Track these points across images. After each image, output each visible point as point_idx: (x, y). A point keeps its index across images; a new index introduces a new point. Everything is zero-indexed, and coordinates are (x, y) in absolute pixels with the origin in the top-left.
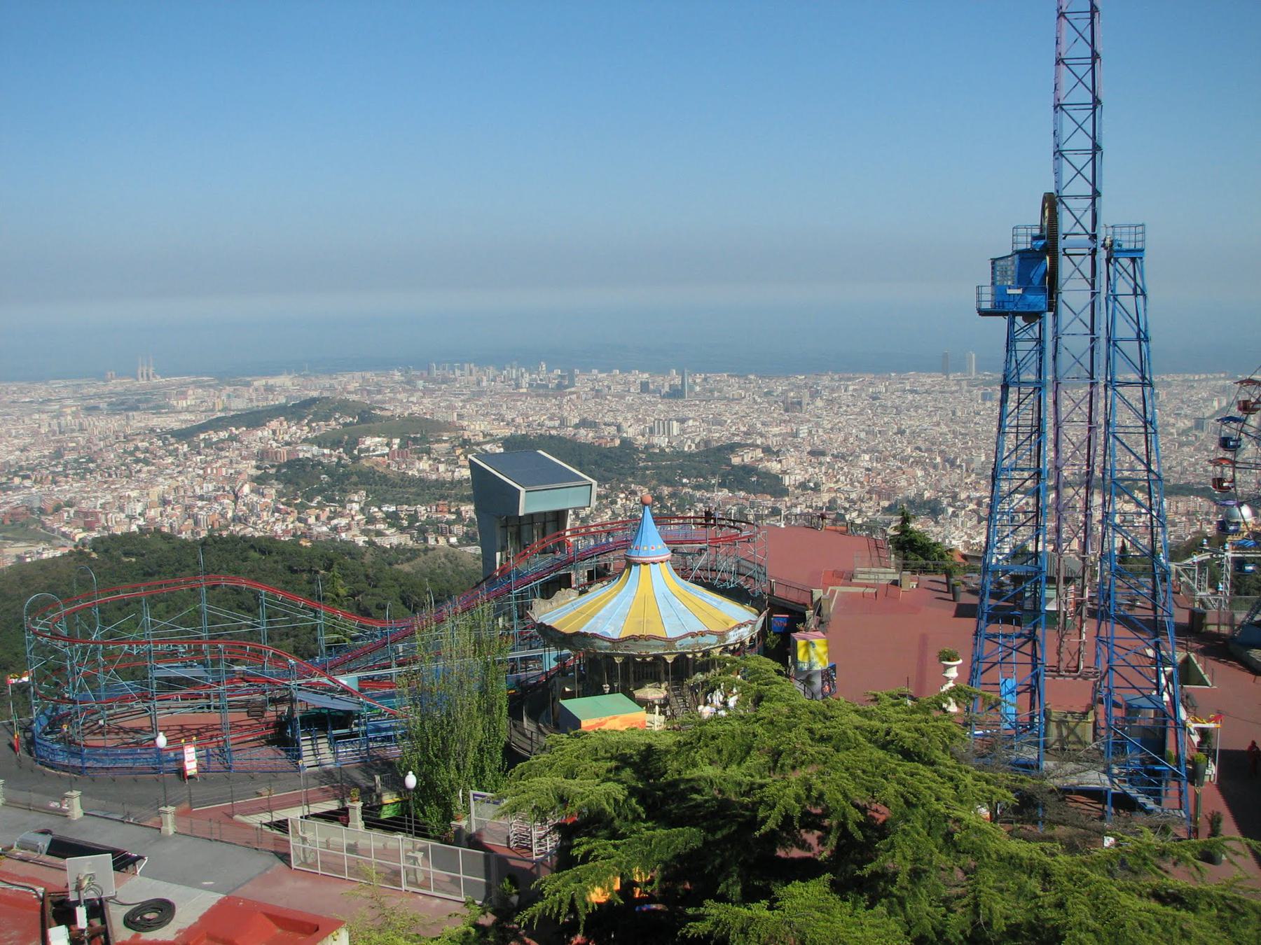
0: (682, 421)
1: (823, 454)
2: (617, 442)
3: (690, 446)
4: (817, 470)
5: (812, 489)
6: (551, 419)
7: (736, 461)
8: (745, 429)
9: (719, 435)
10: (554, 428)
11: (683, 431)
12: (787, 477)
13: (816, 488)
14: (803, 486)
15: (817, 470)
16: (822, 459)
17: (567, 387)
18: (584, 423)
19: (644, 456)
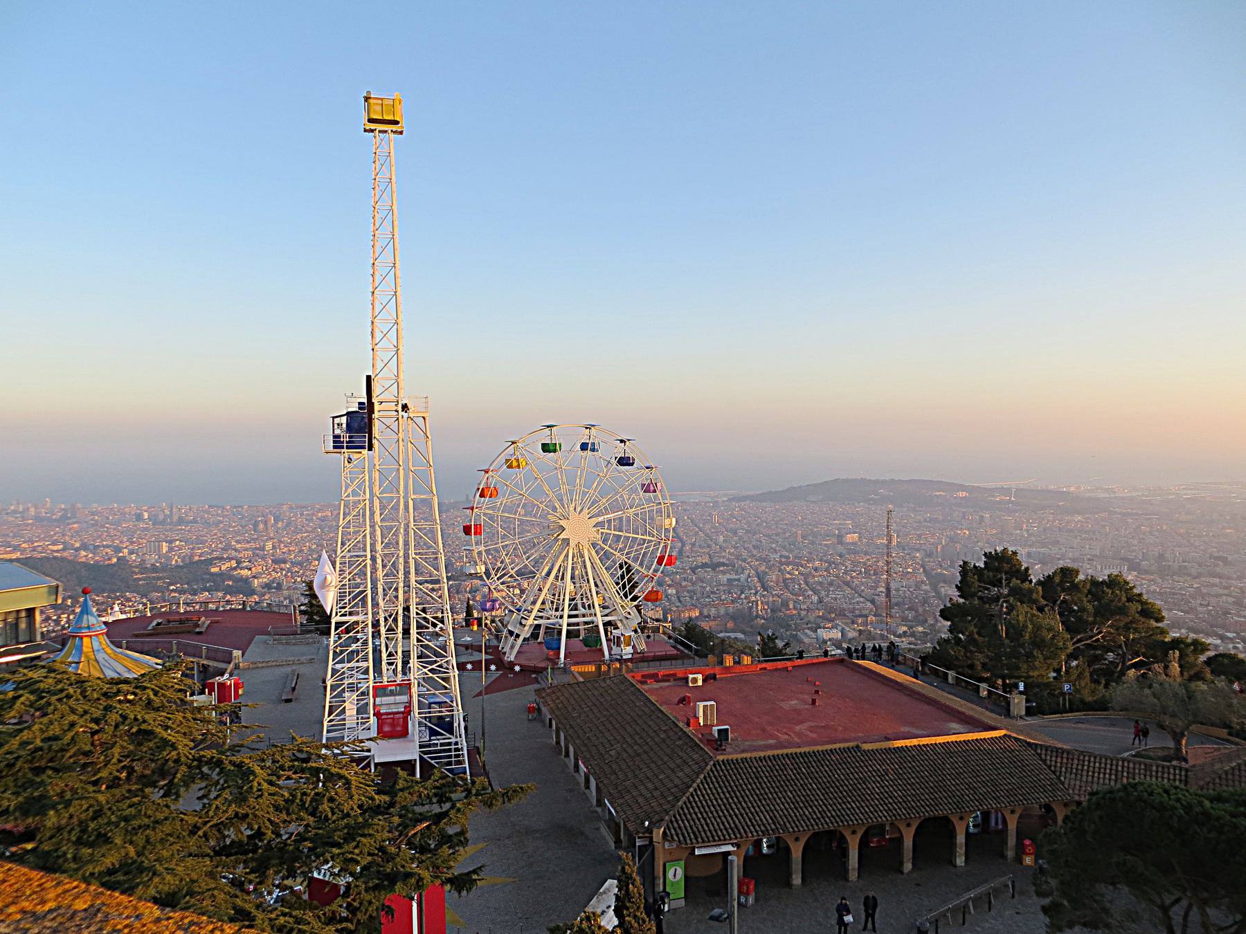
0: (170, 542)
1: (285, 562)
2: (115, 560)
3: (177, 561)
4: (279, 574)
5: (275, 588)
6: (53, 544)
7: (214, 570)
8: (222, 546)
9: (200, 553)
10: (57, 551)
11: (171, 549)
12: (256, 580)
13: (279, 587)
14: (268, 586)
15: (279, 574)
16: (283, 566)
17: (69, 518)
18: (84, 547)
19: (137, 570)
